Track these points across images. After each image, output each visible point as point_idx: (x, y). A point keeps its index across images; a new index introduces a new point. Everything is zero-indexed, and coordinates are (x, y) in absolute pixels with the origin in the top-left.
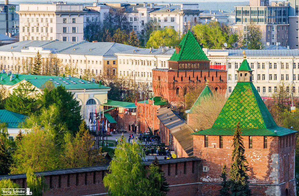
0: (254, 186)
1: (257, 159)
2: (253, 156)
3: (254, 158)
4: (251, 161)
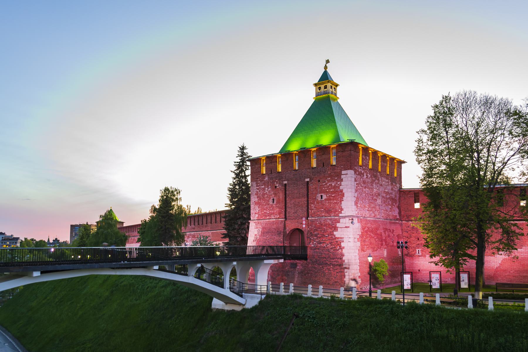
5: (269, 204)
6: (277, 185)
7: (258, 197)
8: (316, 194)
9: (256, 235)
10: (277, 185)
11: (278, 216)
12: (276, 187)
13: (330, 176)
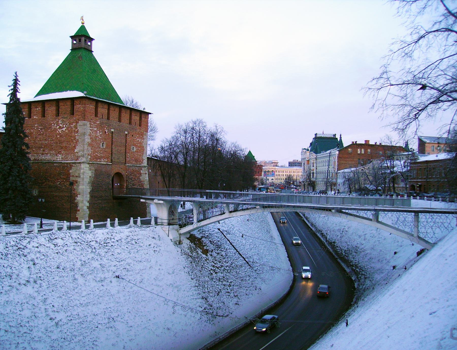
0: (59, 164)
1: (63, 129)
2: (59, 125)
3: (60, 128)
4: (57, 132)
5: (100, 148)
6: (107, 131)
7: (91, 139)
8: (131, 145)
9: (90, 177)
10: (107, 131)
11: (106, 160)
12: (105, 132)
13: (139, 134)
